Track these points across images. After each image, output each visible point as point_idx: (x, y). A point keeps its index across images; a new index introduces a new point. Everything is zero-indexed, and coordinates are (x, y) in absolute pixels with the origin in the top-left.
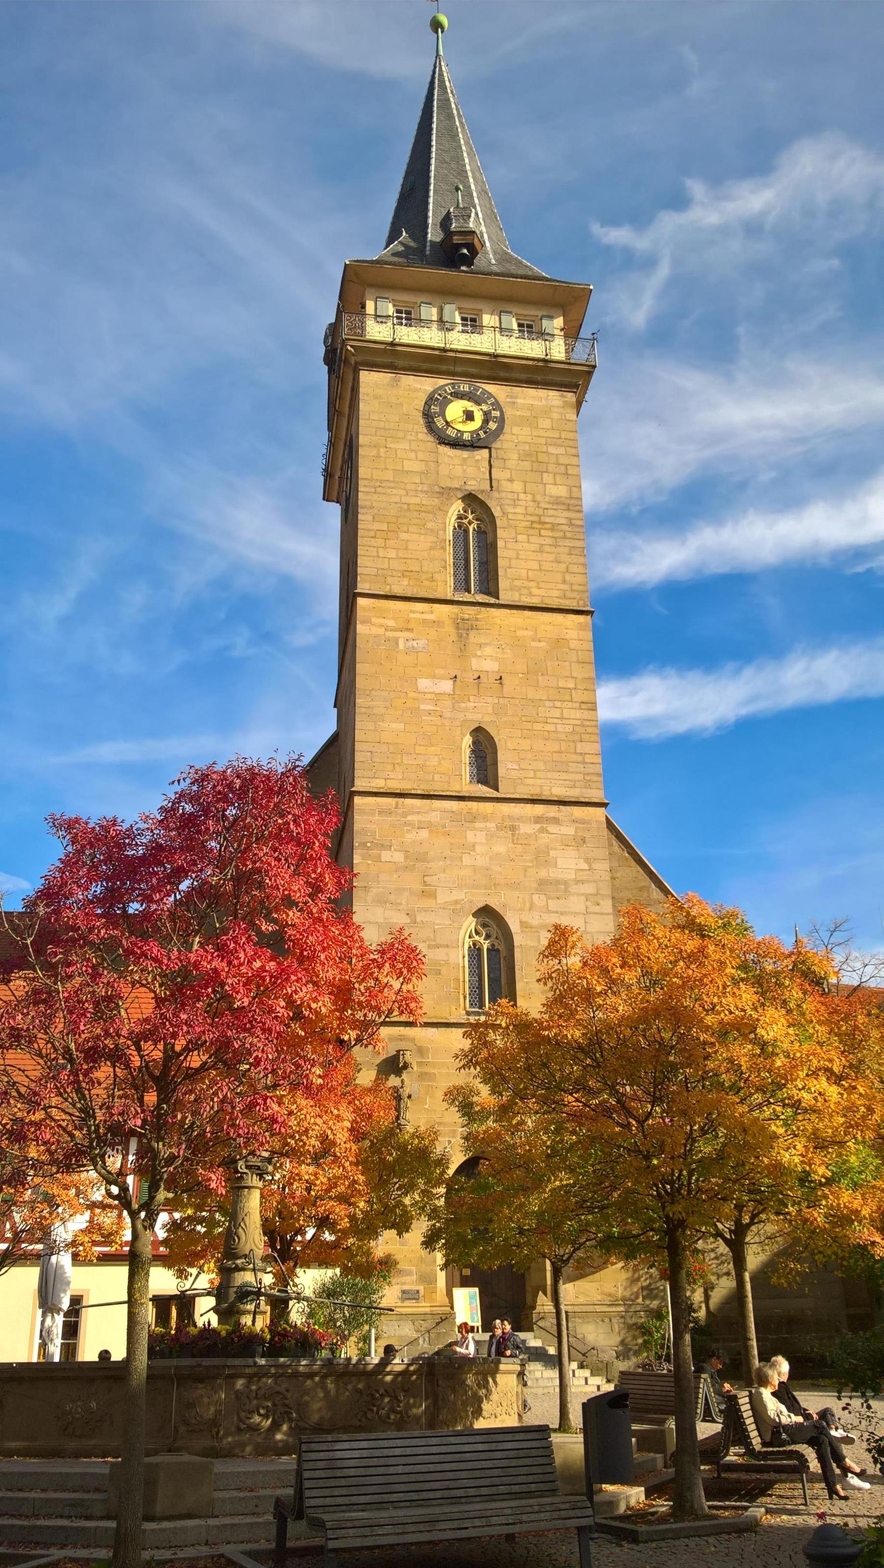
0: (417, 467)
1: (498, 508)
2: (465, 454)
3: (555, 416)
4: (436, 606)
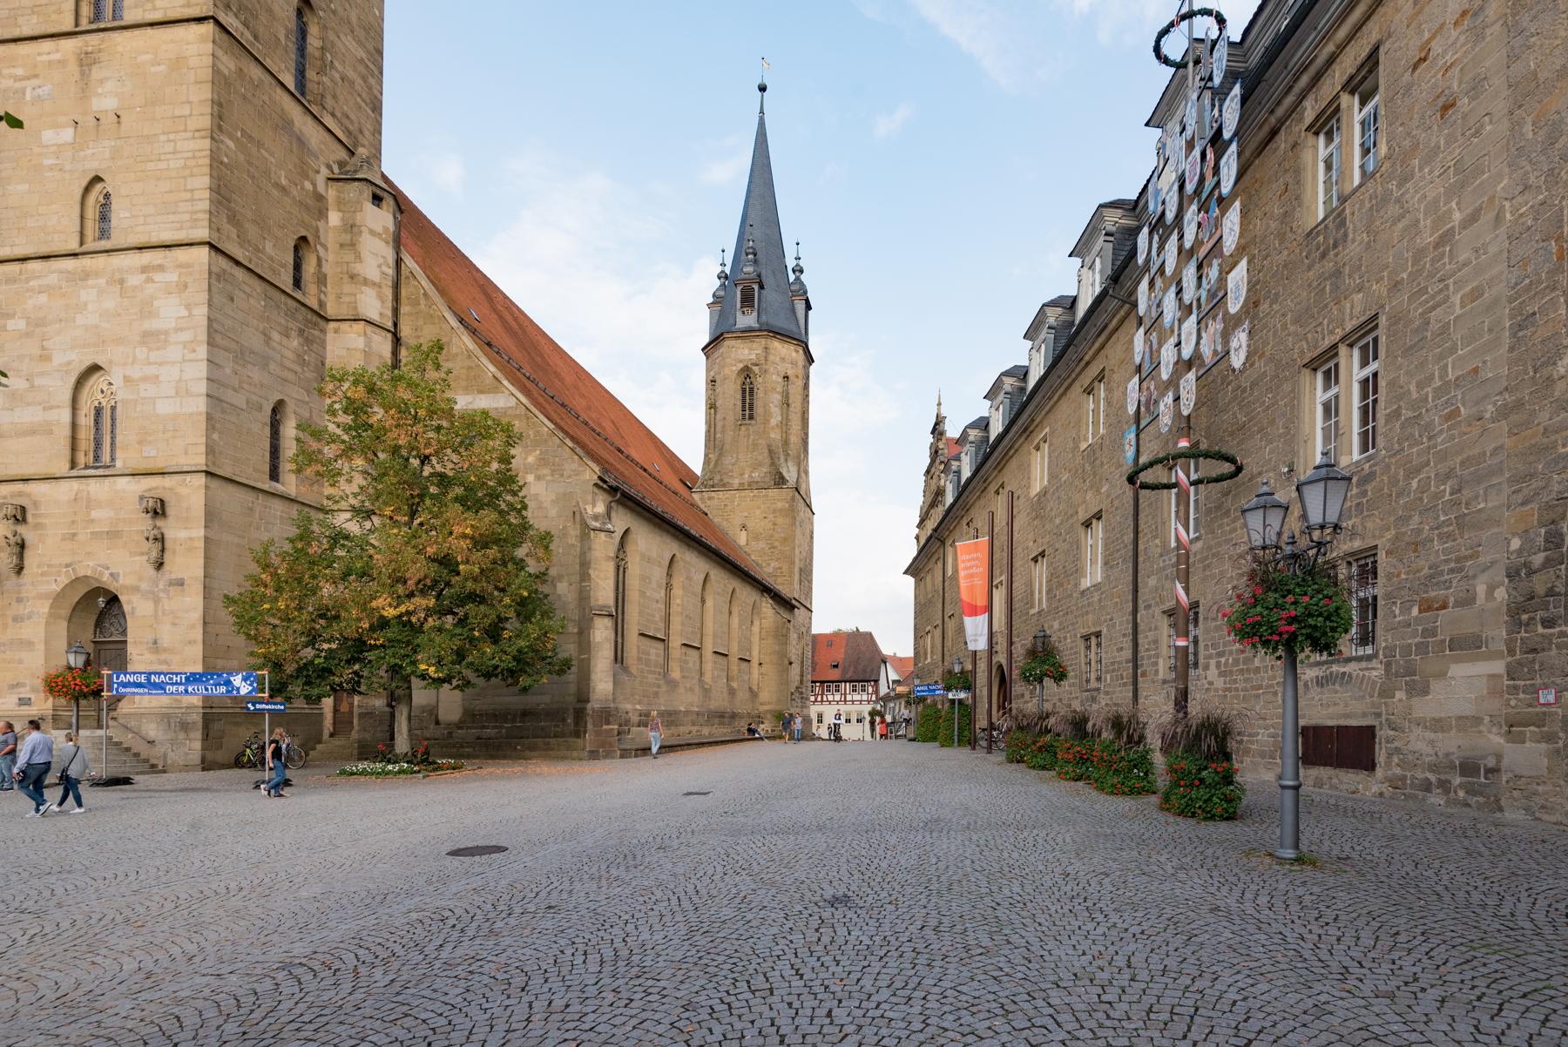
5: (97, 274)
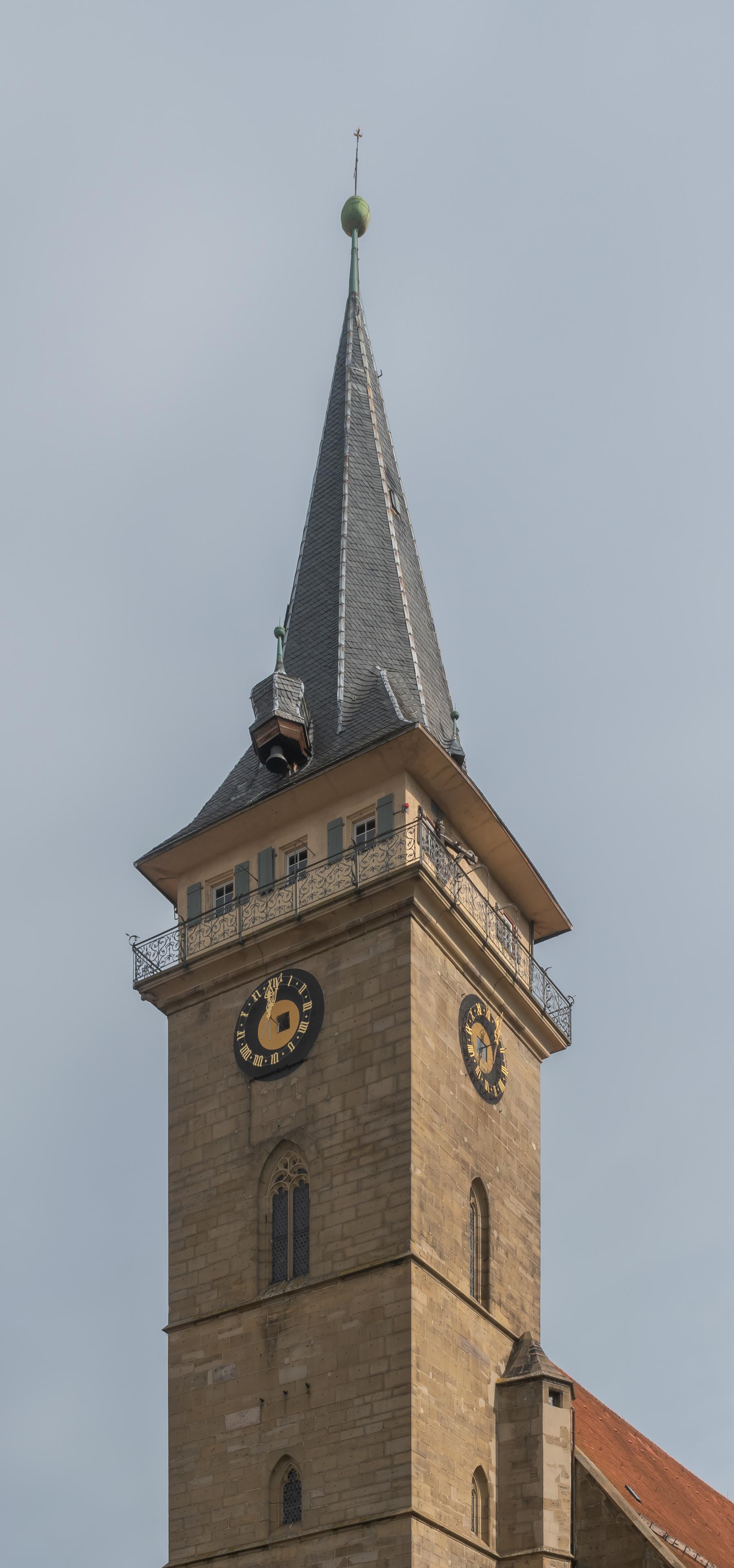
1: (313, 1148)
2: (280, 1083)
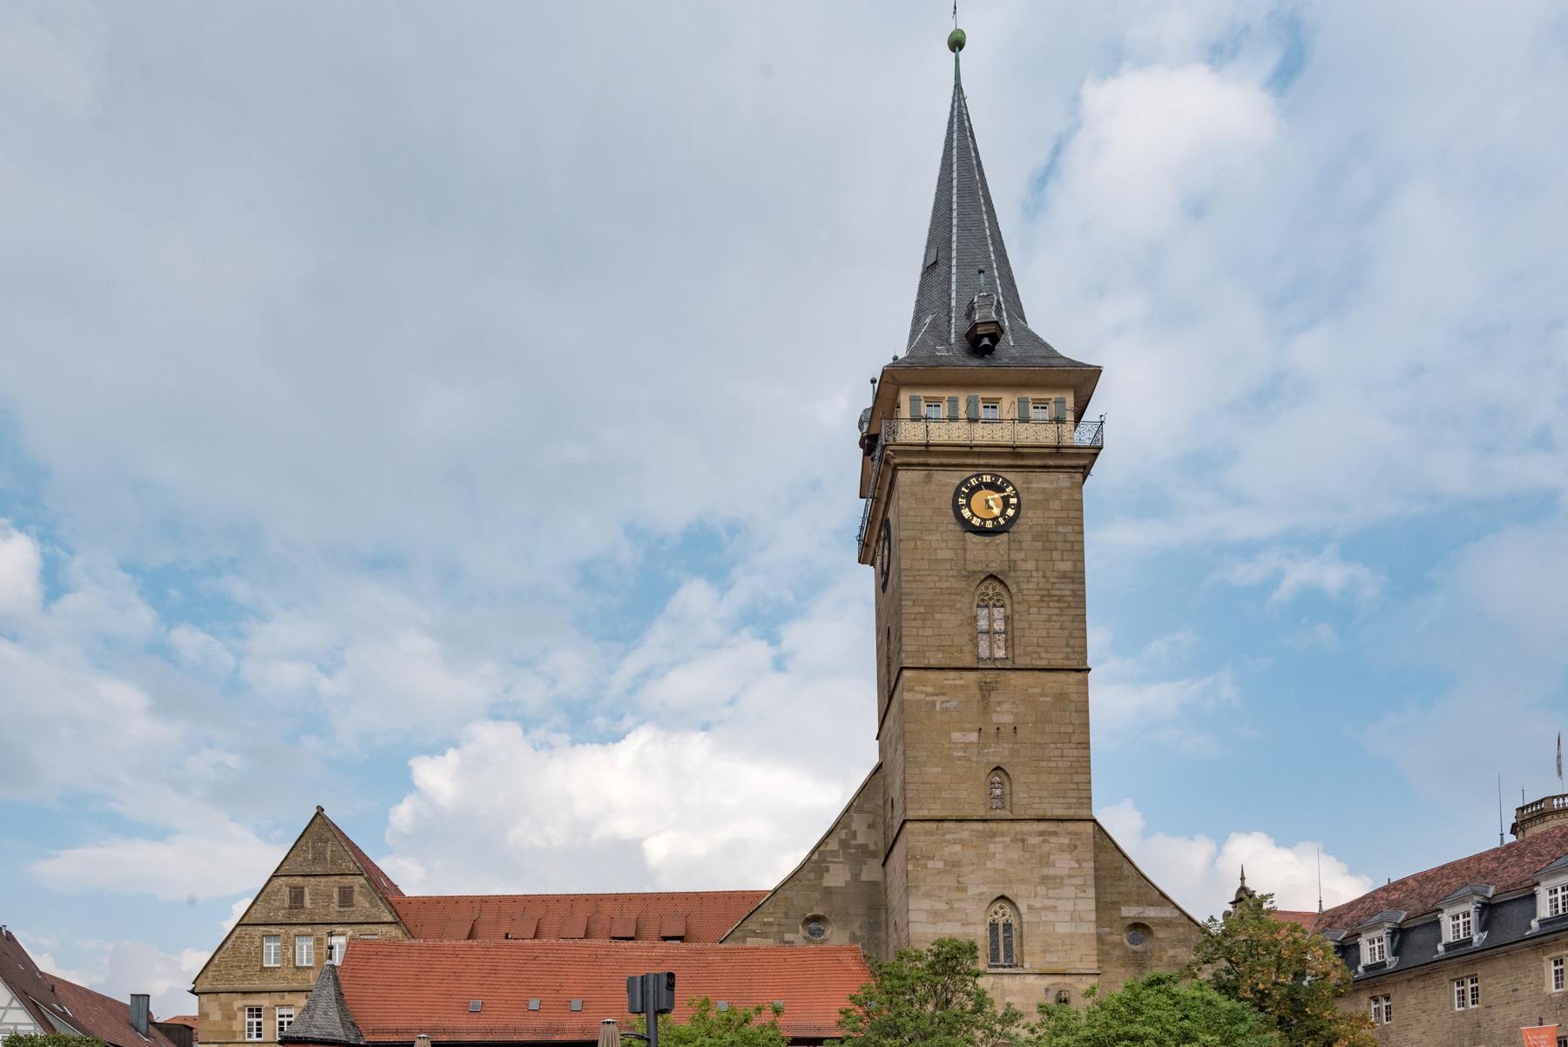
0: (949, 554)
2: (987, 539)
3: (1064, 497)
4: (965, 674)
5: (1003, 834)
